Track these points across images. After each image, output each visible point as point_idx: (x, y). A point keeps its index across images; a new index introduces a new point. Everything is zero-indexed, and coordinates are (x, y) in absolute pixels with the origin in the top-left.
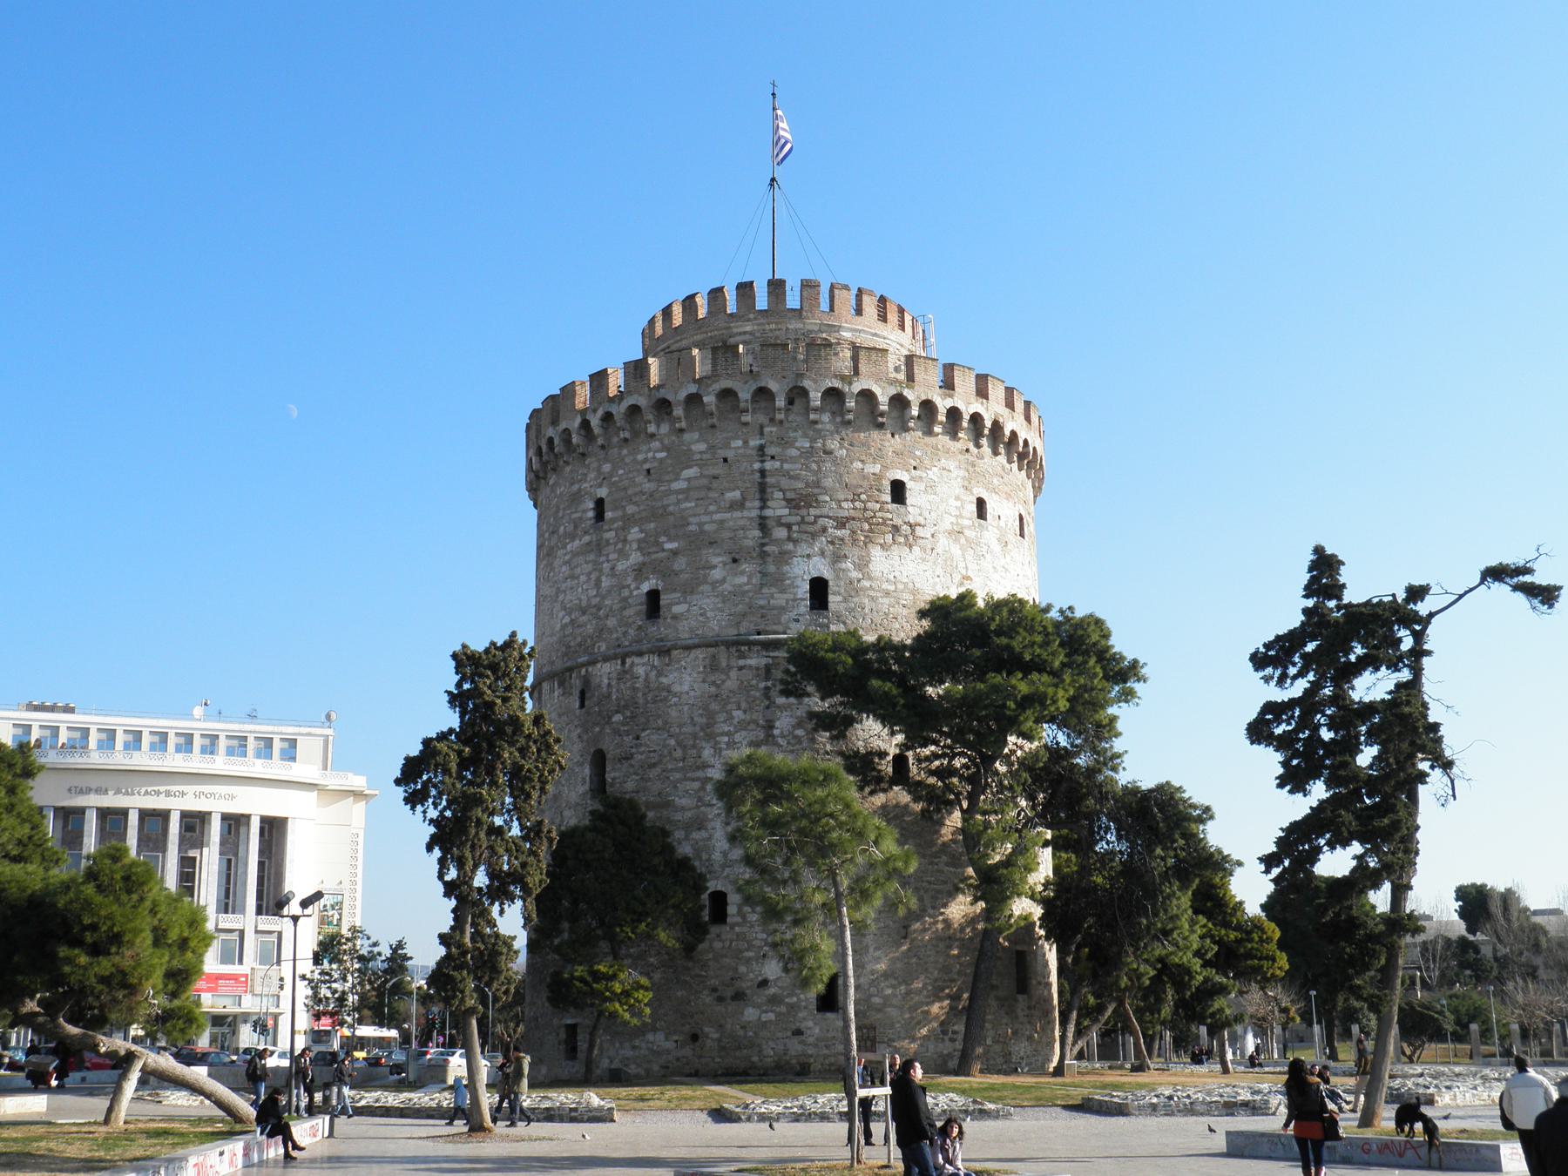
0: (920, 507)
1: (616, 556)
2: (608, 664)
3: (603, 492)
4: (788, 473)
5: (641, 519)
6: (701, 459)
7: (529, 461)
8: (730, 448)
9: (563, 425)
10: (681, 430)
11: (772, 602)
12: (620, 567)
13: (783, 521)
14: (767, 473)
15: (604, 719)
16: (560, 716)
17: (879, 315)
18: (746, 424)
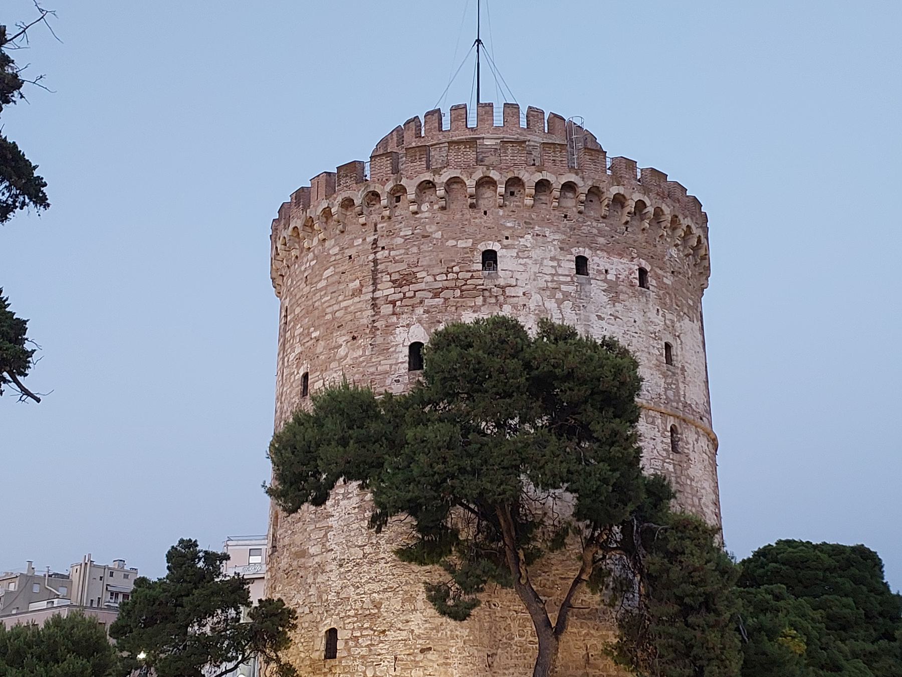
4: (394, 258)
6: (334, 261)
14: (379, 261)
18: (364, 225)
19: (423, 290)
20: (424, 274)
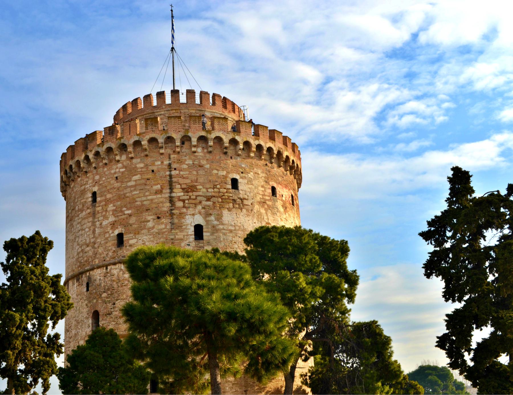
0: (245, 191)
1: (102, 218)
2: (99, 269)
3: (95, 189)
5: (114, 200)
6: (141, 171)
7: (62, 177)
8: (155, 165)
9: (76, 159)
10: (132, 158)
11: (177, 237)
12: (105, 223)
13: (181, 198)
14: (173, 176)
15: (98, 295)
16: (77, 296)
17: (223, 106)
18: (162, 154)
19: (201, 196)
20: (200, 187)
